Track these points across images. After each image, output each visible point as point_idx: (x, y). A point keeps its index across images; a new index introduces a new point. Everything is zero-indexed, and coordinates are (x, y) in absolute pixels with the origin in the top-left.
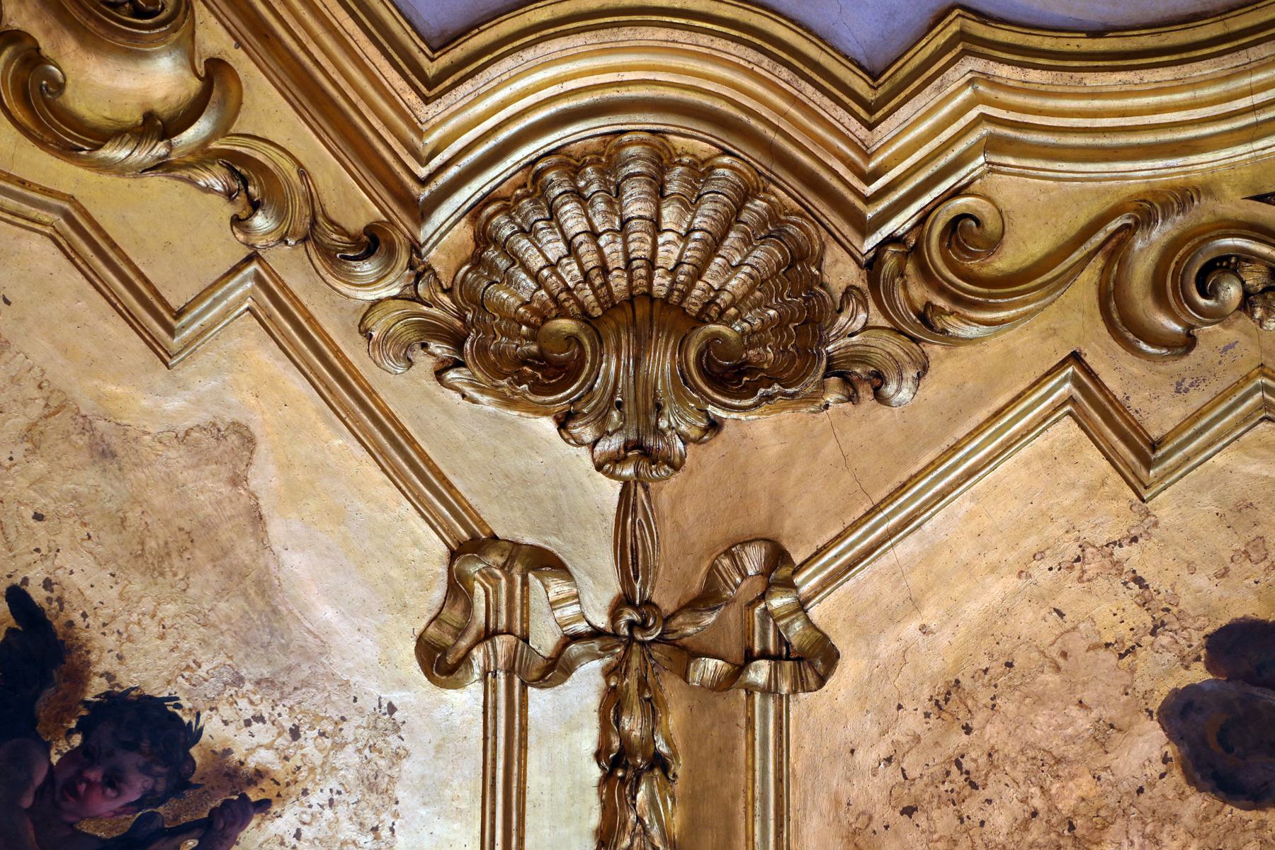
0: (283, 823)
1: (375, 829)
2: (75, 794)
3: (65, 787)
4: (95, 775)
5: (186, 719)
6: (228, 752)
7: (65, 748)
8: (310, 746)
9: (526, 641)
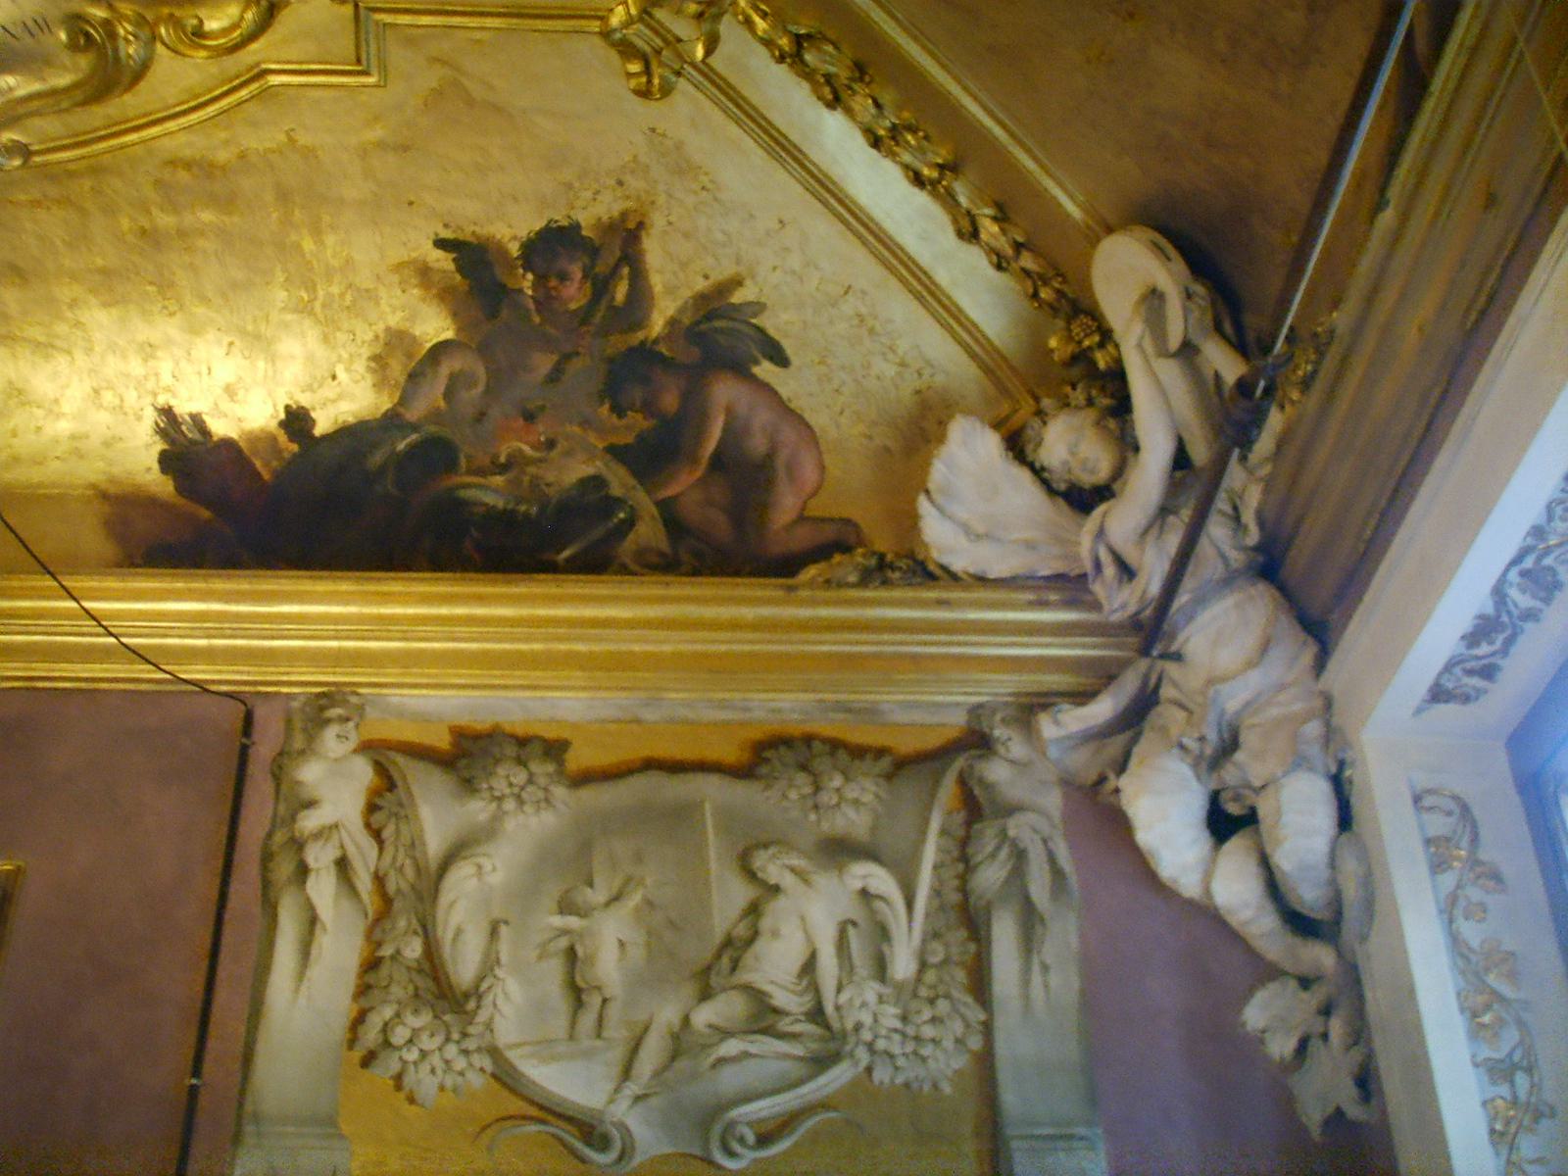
0: (658, 220)
1: (703, 188)
2: (555, 298)
3: (545, 301)
4: (553, 283)
5: (566, 224)
6: (600, 219)
7: (529, 284)
8: (635, 184)
9: (679, 40)
